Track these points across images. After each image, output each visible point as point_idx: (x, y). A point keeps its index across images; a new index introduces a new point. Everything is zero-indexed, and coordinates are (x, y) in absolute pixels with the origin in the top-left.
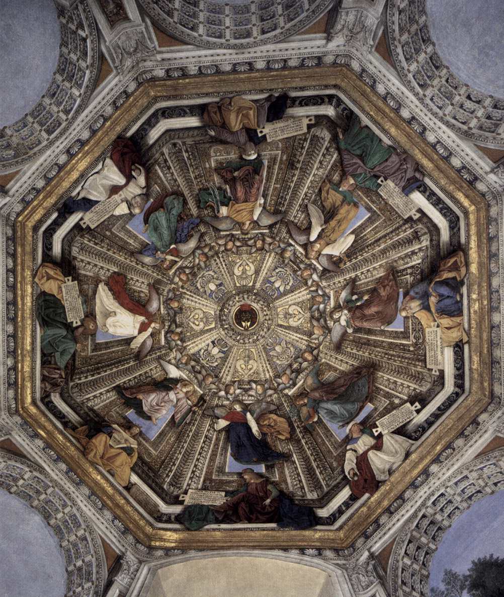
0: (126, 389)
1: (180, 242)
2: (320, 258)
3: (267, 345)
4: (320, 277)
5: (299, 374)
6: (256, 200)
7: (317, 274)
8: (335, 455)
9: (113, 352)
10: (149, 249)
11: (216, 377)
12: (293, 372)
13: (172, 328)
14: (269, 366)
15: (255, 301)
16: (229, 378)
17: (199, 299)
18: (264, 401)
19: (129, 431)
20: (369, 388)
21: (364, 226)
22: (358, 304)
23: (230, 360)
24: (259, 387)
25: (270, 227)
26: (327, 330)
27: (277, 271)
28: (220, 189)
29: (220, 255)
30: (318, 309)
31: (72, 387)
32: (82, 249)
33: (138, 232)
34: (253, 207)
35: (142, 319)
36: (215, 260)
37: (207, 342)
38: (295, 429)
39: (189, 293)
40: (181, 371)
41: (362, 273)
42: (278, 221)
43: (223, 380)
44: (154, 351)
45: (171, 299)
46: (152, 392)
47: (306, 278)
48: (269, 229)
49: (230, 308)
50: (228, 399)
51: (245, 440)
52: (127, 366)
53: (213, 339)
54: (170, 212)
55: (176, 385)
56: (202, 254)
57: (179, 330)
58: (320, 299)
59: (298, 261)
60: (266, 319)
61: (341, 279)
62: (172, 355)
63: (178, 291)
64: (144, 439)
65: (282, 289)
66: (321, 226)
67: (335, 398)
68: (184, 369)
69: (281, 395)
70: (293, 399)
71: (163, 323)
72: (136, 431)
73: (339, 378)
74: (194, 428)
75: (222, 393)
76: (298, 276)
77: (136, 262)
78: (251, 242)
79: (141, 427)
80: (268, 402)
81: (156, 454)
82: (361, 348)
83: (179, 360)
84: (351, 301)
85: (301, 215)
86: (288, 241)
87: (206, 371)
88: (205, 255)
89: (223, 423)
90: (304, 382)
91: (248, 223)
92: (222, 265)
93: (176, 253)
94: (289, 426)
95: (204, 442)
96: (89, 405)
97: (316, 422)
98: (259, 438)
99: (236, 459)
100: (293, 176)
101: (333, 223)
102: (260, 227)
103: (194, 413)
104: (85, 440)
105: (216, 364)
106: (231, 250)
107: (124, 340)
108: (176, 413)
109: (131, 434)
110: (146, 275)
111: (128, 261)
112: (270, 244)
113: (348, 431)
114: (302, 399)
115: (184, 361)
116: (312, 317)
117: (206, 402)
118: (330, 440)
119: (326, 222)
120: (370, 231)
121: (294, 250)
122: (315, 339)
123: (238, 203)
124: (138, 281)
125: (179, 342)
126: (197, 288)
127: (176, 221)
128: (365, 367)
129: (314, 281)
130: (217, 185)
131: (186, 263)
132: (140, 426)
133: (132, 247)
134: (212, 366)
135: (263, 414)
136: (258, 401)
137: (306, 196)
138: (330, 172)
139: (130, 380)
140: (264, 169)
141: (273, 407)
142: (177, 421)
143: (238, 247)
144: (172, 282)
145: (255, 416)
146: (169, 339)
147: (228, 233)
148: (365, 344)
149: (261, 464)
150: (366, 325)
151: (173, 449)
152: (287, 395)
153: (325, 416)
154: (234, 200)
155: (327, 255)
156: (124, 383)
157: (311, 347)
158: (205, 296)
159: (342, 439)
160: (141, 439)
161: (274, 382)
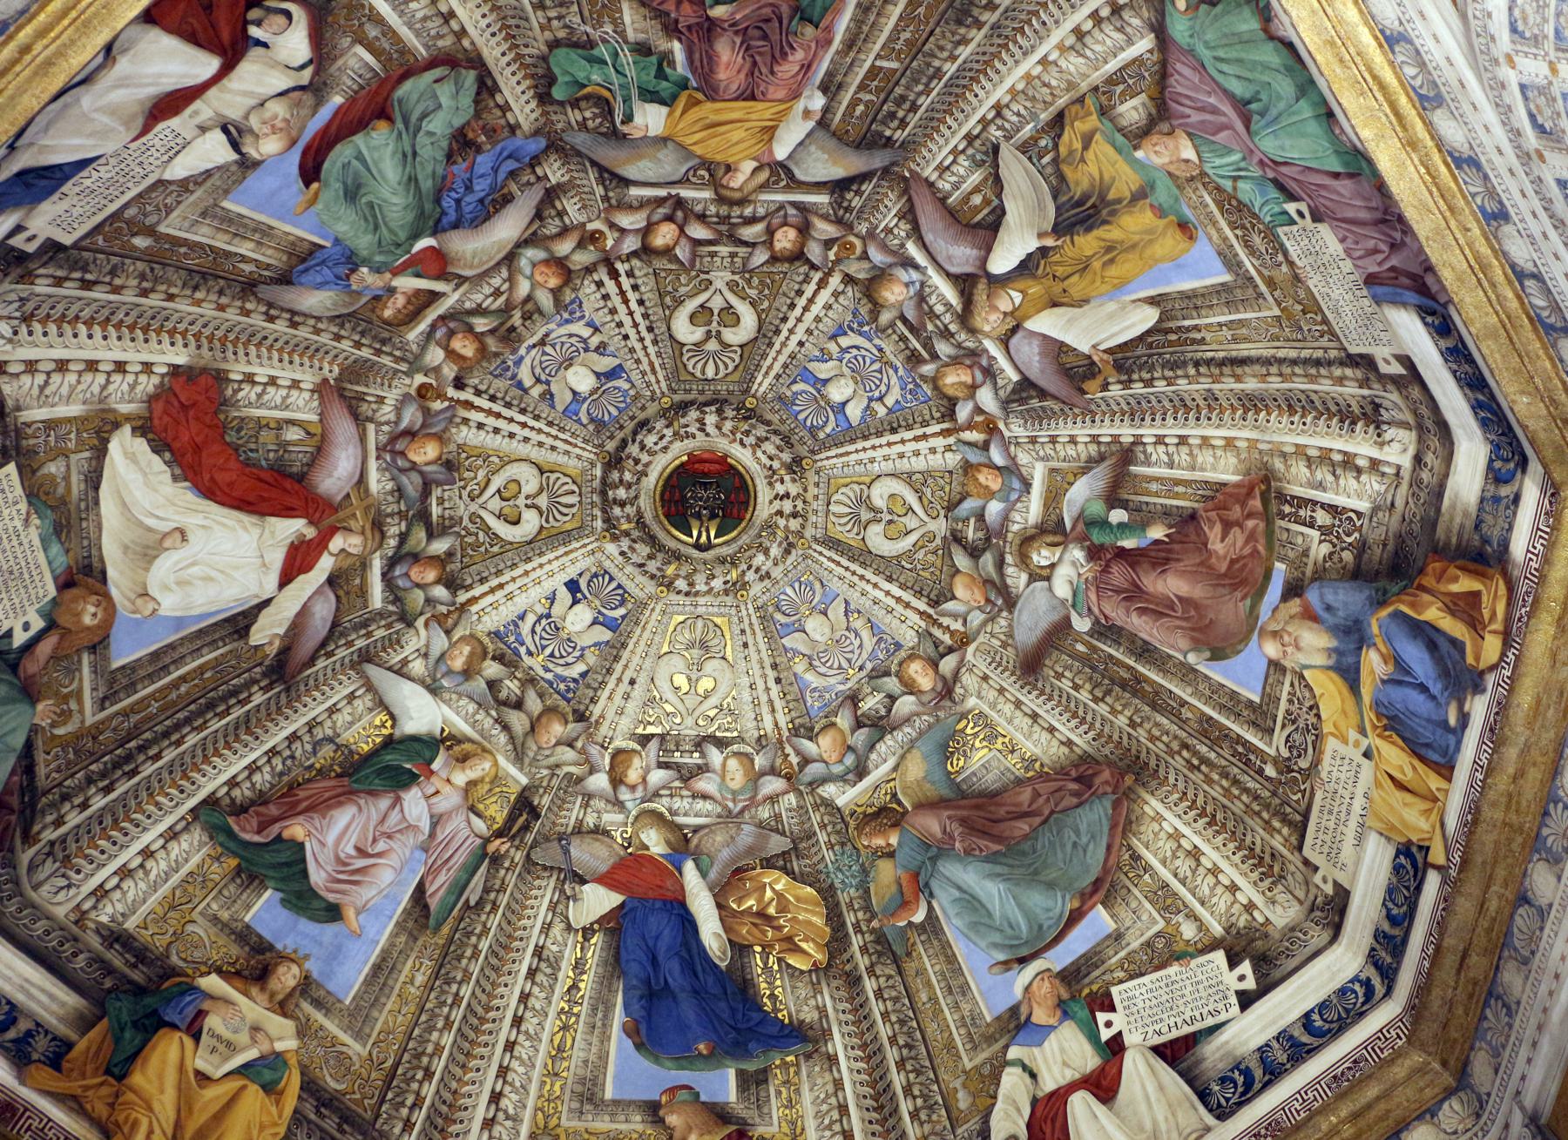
0: (240, 810)
1: (456, 226)
2: (1014, 341)
3: (778, 608)
4: (1005, 404)
5: (881, 738)
6: (795, 95)
7: (996, 389)
8: (969, 1065)
9: (183, 679)
10: (323, 262)
11: (581, 717)
12: (859, 724)
13: (411, 544)
14: (775, 690)
15: (747, 441)
16: (625, 724)
17: (524, 425)
18: (747, 815)
19: (263, 989)
20: (1109, 847)
22: (1129, 543)
23: (633, 656)
24: (733, 764)
25: (839, 187)
26: (1004, 598)
27: (845, 342)
28: (642, 49)
29: (619, 266)
30: (980, 516)
31: (32, 867)
32: (27, 319)
33: (272, 216)
34: (780, 117)
35: (294, 528)
36: (600, 284)
37: (548, 586)
38: (847, 935)
39: (486, 404)
40: (448, 702)
43: (604, 729)
44: (342, 635)
45: (410, 434)
46: (340, 804)
47: (950, 392)
49: (645, 458)
50: (619, 805)
51: (673, 971)
52: (237, 712)
53: (571, 573)
54: (419, 129)
55: (432, 760)
56: (546, 262)
57: (440, 546)
58: (987, 479)
59: (930, 327)
60: (780, 513)
61: (1082, 432)
62: (413, 642)
63: (441, 396)
64: (318, 1004)
65: (854, 412)
66: (1040, 235)
67: (995, 853)
68: (460, 695)
69: (809, 799)
70: (852, 824)
71: (378, 526)
72: (287, 978)
73: (1019, 782)
74: (495, 921)
75: (600, 781)
76: (922, 377)
77: (266, 313)
78: (749, 233)
79: (307, 957)
80: (760, 825)
81: (365, 1053)
82: (1108, 692)
83: (443, 655)
84: (1104, 524)
87: (541, 696)
88: (560, 264)
89: (598, 901)
90: (895, 769)
91: (748, 166)
92: (626, 301)
93: (438, 264)
94: (829, 919)
95: (532, 973)
96: (104, 919)
97: (921, 928)
98: (723, 965)
99: (639, 1046)
100: (959, 43)
101: (1087, 243)
102: (795, 184)
103: (496, 860)
104: (105, 1091)
105: (581, 668)
106: (667, 252)
107: (226, 620)
108: (432, 871)
109: (272, 995)
110: (312, 352)
111: (232, 315)
113: (1018, 992)
114: (881, 831)
115: (458, 663)
116: (957, 538)
117: (538, 816)
118: (957, 1007)
119: (1059, 230)
121: (922, 284)
122: (955, 616)
123: (714, 100)
124: (273, 381)
125: (440, 592)
126: (520, 385)
127: (440, 156)
128: (1110, 764)
129: (978, 410)
130: (631, 35)
131: (478, 298)
132: (301, 953)
133: (247, 268)
134: (564, 679)
135: (738, 871)
136: (729, 818)
137: (999, 114)
138: (1111, 81)
139: (253, 768)
140: (839, 12)
141: (777, 844)
142: (434, 903)
143: (697, 243)
144: (415, 363)
145: (713, 875)
146: (400, 583)
147: (662, 193)
148: (1124, 685)
149: (720, 1065)
150: (1141, 626)
151: (423, 1018)
152: (828, 804)
153: (951, 912)
154: (697, 89)
155: (1045, 337)
156: (232, 783)
157: (936, 645)
158: (544, 410)
159: (996, 1014)
160: (307, 1007)
161: (789, 750)
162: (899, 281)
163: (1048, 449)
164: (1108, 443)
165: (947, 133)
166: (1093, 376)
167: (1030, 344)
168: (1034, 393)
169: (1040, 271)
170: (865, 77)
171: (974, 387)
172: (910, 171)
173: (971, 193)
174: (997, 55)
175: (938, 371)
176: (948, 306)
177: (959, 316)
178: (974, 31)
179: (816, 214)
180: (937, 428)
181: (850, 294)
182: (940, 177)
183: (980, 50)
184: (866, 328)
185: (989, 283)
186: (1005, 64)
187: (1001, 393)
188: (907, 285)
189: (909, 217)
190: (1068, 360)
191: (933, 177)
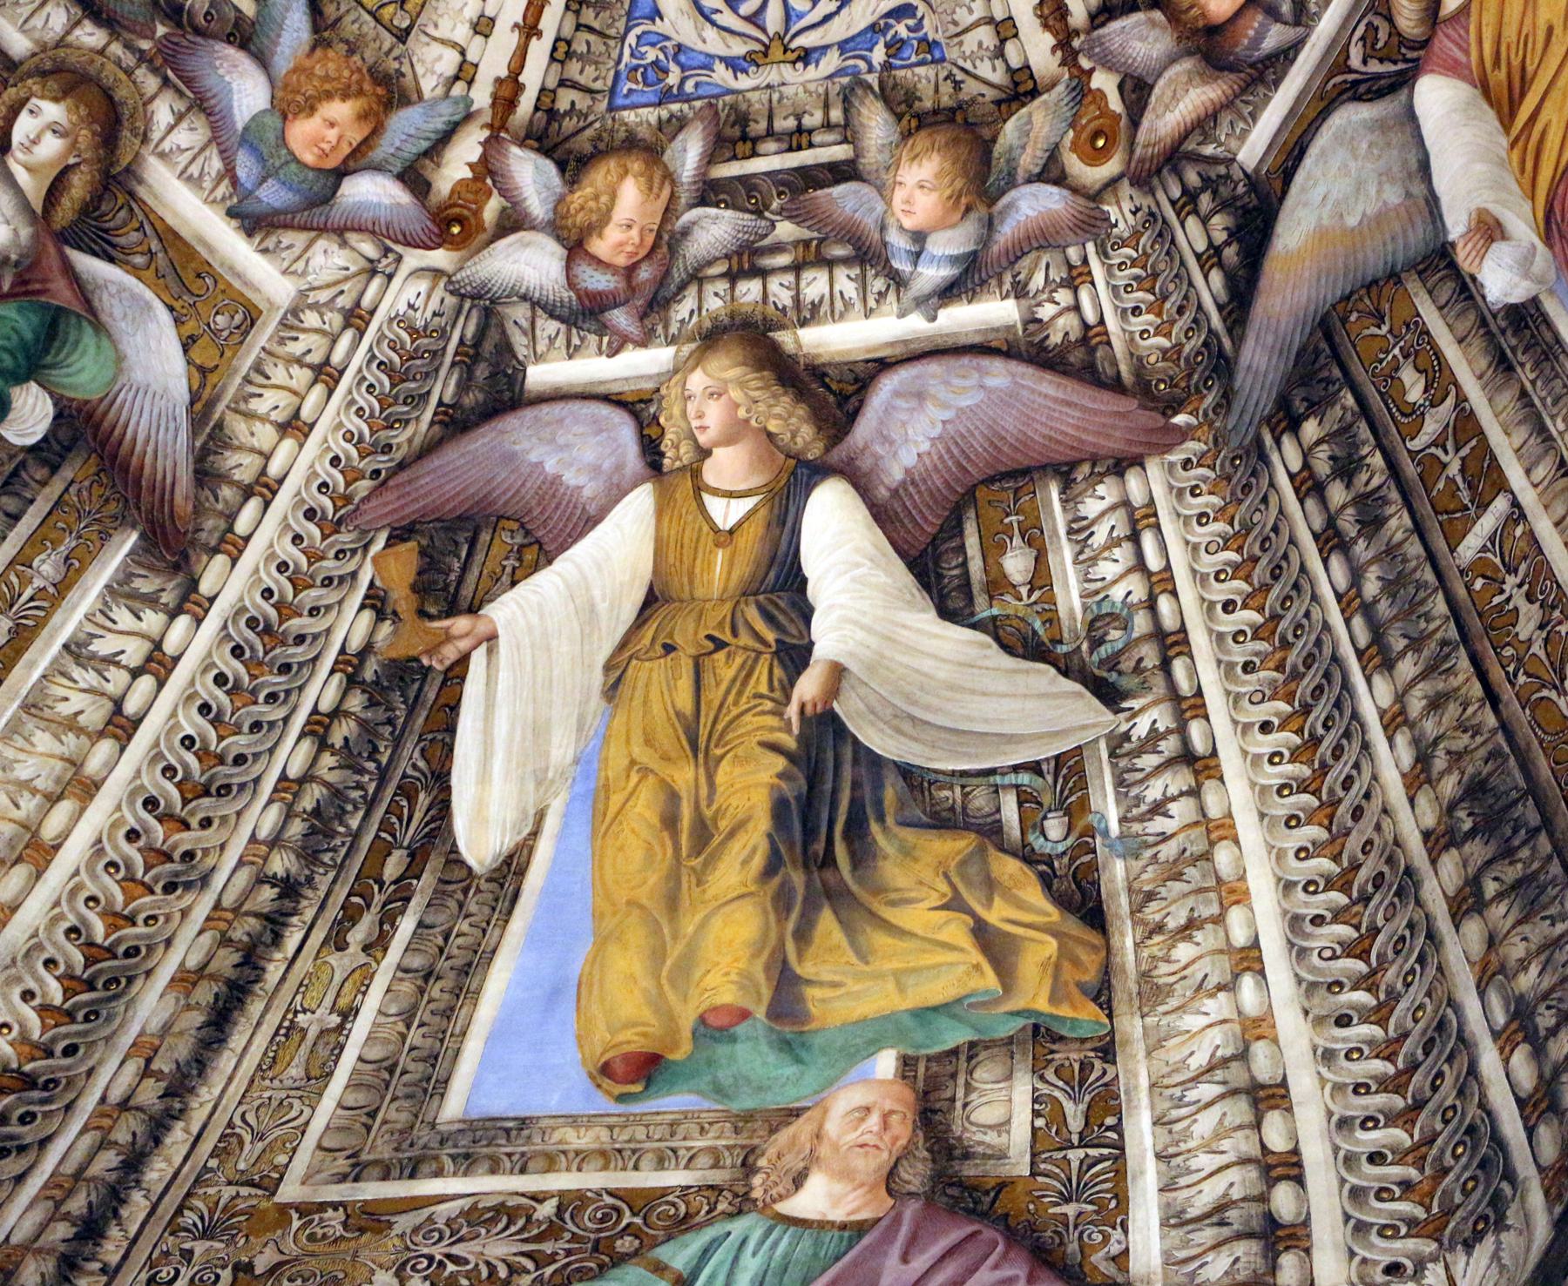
2: (625, 431)
7: (538, 304)
21: (435, 990)
41: (158, 664)
42: (1238, 342)
48: (1252, 180)
85: (1094, 593)
86: (1020, 291)
112: (1137, 90)
120: (349, 1014)
121: (898, 281)
129: (513, 222)
162: (942, 225)
163: (309, 344)
164: (231, 518)
165: (1219, 592)
166: (421, 588)
167: (596, 469)
168: (469, 400)
169: (752, 614)
170: (1485, 449)
171: (575, 247)
172: (1185, 434)
173: (1040, 559)
174: (1333, 846)
175: (669, 177)
176: (808, 314)
177: (770, 325)
178: (1429, 820)
179: (1228, 105)
180: (534, 75)
181: (985, 69)
182: (1126, 503)
183: (1374, 806)
184: (879, 55)
185: (801, 462)
186: (1302, 853)
187: (520, 313)
188: (919, 237)
189: (1077, 357)
190: (500, 545)
191: (1133, 481)
